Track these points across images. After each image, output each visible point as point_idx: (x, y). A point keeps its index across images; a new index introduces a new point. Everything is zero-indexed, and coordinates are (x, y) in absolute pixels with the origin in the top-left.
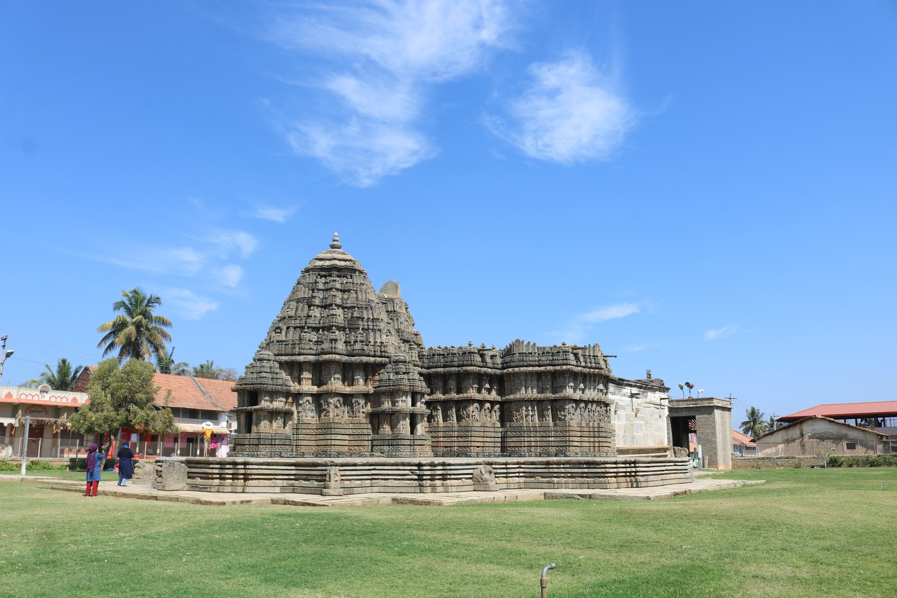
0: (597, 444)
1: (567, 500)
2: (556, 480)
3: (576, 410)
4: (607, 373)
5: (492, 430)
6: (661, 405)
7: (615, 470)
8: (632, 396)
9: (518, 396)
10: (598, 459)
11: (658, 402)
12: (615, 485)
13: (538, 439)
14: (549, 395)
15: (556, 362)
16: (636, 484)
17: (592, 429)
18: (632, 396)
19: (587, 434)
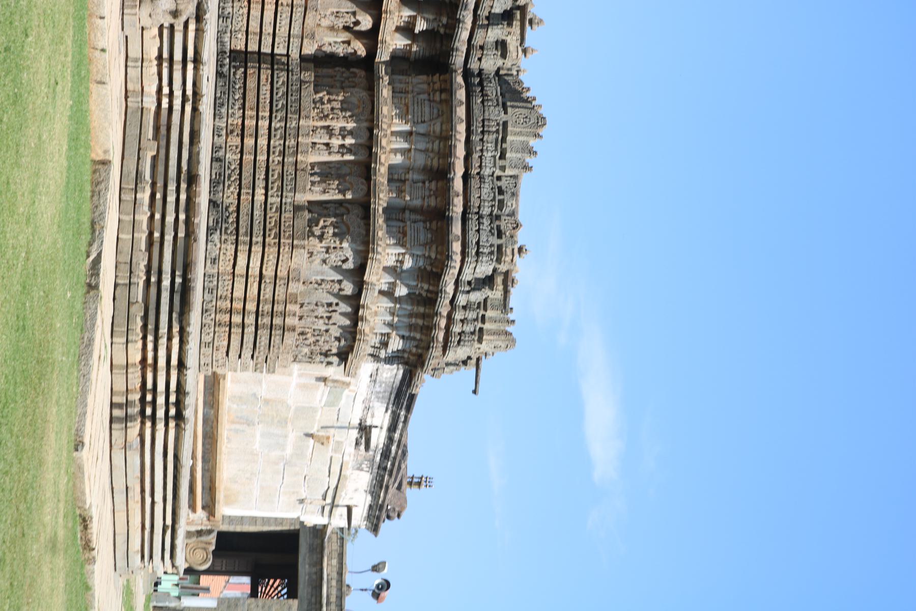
0: (237, 319)
1: (86, 221)
2: (145, 196)
3: (337, 269)
4: (433, 363)
5: (296, 30)
6: (333, 505)
7: (162, 362)
8: (365, 430)
9: (386, 109)
10: (195, 317)
11: (344, 499)
12: (120, 360)
13: (262, 158)
14: (383, 198)
15: (473, 225)
16: (119, 415)
17: (279, 308)
18: (365, 430)
19: (267, 293)
